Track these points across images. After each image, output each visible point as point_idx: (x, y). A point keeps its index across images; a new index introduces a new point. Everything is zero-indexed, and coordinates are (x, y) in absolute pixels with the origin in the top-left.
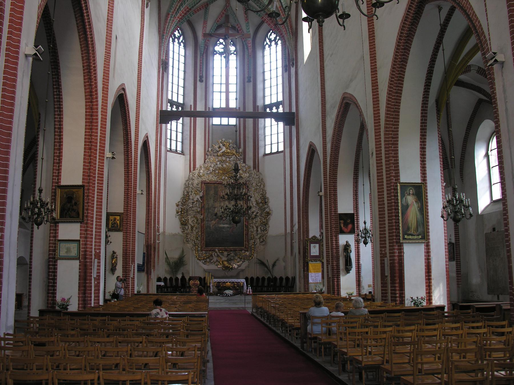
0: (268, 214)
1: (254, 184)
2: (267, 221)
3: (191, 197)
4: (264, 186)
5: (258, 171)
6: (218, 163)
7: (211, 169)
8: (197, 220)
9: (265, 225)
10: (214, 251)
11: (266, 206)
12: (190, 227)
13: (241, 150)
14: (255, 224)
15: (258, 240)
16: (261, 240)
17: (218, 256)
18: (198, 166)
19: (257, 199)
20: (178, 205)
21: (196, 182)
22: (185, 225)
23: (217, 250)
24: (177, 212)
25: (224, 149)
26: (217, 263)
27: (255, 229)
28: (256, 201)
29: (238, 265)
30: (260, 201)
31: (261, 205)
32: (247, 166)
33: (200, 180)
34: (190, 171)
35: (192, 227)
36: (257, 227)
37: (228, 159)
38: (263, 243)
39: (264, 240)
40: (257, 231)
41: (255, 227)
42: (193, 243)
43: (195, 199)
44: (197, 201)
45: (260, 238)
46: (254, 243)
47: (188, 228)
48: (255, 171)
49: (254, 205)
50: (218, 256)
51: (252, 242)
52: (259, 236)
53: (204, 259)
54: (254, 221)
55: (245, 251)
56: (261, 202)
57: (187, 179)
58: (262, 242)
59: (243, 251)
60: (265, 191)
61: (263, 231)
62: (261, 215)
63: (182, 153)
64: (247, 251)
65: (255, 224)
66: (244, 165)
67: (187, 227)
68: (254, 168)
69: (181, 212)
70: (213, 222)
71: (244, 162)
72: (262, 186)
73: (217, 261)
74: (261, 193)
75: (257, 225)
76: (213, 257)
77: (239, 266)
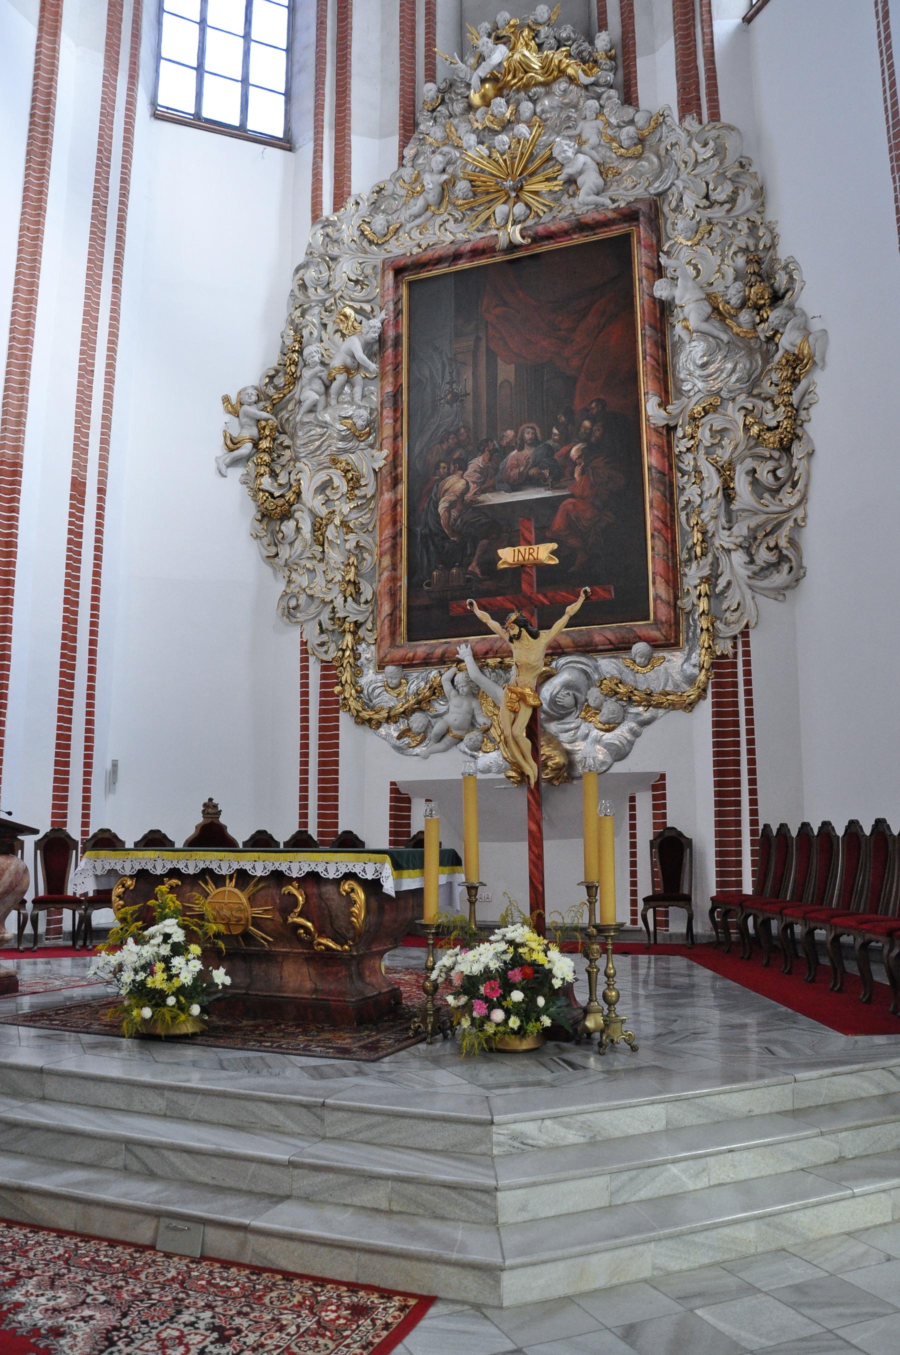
0: (798, 365)
1: (689, 202)
2: (795, 414)
3: (313, 351)
4: (760, 194)
5: (715, 115)
6: (473, 138)
7: (431, 181)
8: (354, 483)
9: (786, 449)
10: (448, 660)
11: (774, 315)
12: (306, 528)
13: (602, 40)
14: (709, 451)
15: (739, 557)
16: (763, 556)
17: (475, 692)
18: (361, 183)
19: (718, 288)
20: (233, 408)
21: (347, 268)
22: (287, 516)
23: (464, 652)
24: (233, 444)
25: (499, 54)
26: (474, 736)
27: (713, 482)
28: (710, 298)
29: (608, 746)
30: (734, 293)
31: (745, 317)
32: (640, 119)
33: (378, 256)
34: (316, 216)
35: (319, 527)
36: (726, 471)
37: (526, 107)
38: (780, 578)
39: (783, 558)
40: (728, 493)
41: (708, 470)
42: (325, 617)
43: (337, 362)
44: (349, 371)
45: (748, 547)
46: (711, 580)
47: (298, 529)
48: (691, 123)
49: (694, 322)
50: (475, 692)
51: (693, 574)
52: (741, 529)
53: (390, 719)
54: (704, 435)
55: (656, 645)
57: (301, 259)
58: (774, 566)
59: (640, 648)
61: (775, 492)
62: (752, 384)
63: (286, 143)
64: (671, 644)
65: (709, 451)
66: (628, 112)
67: (288, 527)
69: (256, 445)
70: (455, 483)
71: (629, 97)
72: (745, 201)
73: (472, 725)
74: (741, 240)
75: (723, 455)
76: (444, 697)
77: (620, 753)
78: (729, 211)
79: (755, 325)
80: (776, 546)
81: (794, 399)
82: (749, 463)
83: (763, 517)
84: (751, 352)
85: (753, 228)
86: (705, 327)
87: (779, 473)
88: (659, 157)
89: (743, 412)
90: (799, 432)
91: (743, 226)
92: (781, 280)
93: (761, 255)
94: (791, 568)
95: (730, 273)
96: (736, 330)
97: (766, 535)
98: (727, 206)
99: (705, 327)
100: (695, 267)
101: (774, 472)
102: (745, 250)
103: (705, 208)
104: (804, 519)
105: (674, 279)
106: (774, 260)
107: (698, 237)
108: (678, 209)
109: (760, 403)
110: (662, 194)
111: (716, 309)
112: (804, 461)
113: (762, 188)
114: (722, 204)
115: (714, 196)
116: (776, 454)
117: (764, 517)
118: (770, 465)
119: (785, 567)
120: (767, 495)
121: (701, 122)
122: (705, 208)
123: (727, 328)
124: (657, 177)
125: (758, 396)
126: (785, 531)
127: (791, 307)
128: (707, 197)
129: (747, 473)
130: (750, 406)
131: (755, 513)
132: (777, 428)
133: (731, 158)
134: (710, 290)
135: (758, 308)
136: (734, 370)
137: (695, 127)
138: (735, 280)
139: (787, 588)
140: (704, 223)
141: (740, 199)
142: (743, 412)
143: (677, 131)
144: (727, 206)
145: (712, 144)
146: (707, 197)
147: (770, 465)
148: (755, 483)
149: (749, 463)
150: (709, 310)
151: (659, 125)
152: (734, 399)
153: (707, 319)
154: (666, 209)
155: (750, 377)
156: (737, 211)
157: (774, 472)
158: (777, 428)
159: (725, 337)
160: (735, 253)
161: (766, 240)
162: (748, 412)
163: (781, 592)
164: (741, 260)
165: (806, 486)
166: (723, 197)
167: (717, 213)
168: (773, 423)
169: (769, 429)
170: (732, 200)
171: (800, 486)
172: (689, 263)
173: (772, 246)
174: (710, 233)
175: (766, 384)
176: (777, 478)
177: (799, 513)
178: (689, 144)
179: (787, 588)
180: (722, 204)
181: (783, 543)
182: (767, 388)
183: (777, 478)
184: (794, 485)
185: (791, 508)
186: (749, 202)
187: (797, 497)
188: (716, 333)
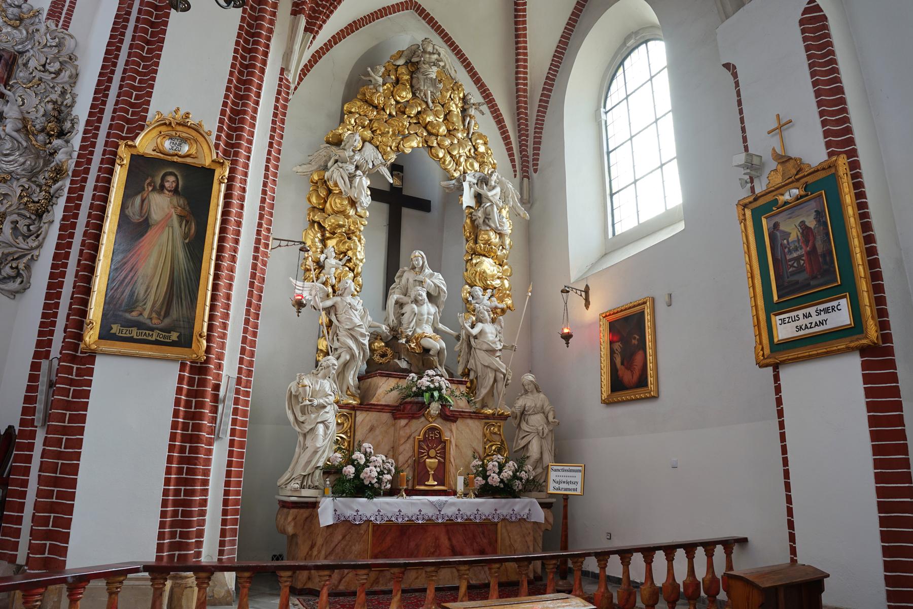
1: (33, 64)
5: (66, 26)
9: (40, 216)
11: (57, 142)
28: (24, 120)
31: (41, 137)
38: (14, 285)
39: (19, 274)
48: (51, 24)
56: (43, 130)
60: (74, 97)
61: (26, 237)
62: (32, 175)
68: (54, 14)
72: (65, 76)
74: (54, 97)
78: (53, 78)
79: (46, 144)
80: (17, 268)
81: (52, 191)
82: (15, 217)
83: (15, 249)
84: (38, 157)
85: (63, 93)
86: (15, 134)
87: (31, 227)
88: (27, 33)
89: (21, 188)
90: (49, 208)
91: (59, 89)
92: (68, 125)
93: (63, 108)
94: (22, 282)
95: (42, 111)
96: (34, 142)
97: (13, 260)
98: (53, 75)
99: (15, 134)
100: (23, 100)
101: (28, 226)
102: (55, 103)
103: (40, 71)
104: (37, 256)
105: (8, 101)
106: (69, 114)
107: (30, 85)
108: (25, 65)
109: (34, 187)
110: (21, 53)
111: (25, 127)
112: (47, 225)
113: (77, 75)
114: (51, 73)
115: (47, 67)
116: (33, 217)
117: (15, 249)
118: (27, 222)
119: (19, 280)
120: (20, 238)
121: (57, 26)
122: (40, 71)
123: (28, 140)
124: (22, 43)
125: (34, 182)
126: (25, 260)
127: (67, 142)
128: (44, 66)
129: (12, 222)
130: (27, 186)
131: (11, 246)
132: (38, 202)
133: (65, 51)
134: (27, 116)
135: (50, 136)
136: (24, 163)
137: (53, 27)
138: (43, 116)
139: (17, 292)
140: (37, 78)
141: (62, 74)
142: (21, 188)
143: (44, 24)
144: (53, 75)
145: (57, 40)
146: (44, 66)
147: (27, 222)
148: (15, 229)
149: (15, 217)
150: (20, 126)
151: (35, 16)
152: (18, 180)
153: (18, 131)
154: (20, 61)
155: (32, 170)
156: (58, 80)
157: (28, 226)
158: (38, 202)
159: (25, 144)
160: (48, 102)
161: (68, 101)
162: (24, 189)
163: (13, 294)
164: (50, 106)
165: (44, 239)
166: (52, 70)
167: (47, 77)
168: (36, 199)
169: (34, 202)
170: (58, 73)
171: (40, 238)
172: (20, 96)
173: (71, 106)
174: (38, 85)
175: (41, 177)
176: (29, 230)
177: (36, 253)
178: (45, 34)
179: (17, 292)
180: (51, 73)
181: (21, 266)
182: (41, 179)
183: (29, 230)
184: (37, 237)
185: (32, 249)
186: (66, 79)
187: (36, 243)
188: (20, 140)
